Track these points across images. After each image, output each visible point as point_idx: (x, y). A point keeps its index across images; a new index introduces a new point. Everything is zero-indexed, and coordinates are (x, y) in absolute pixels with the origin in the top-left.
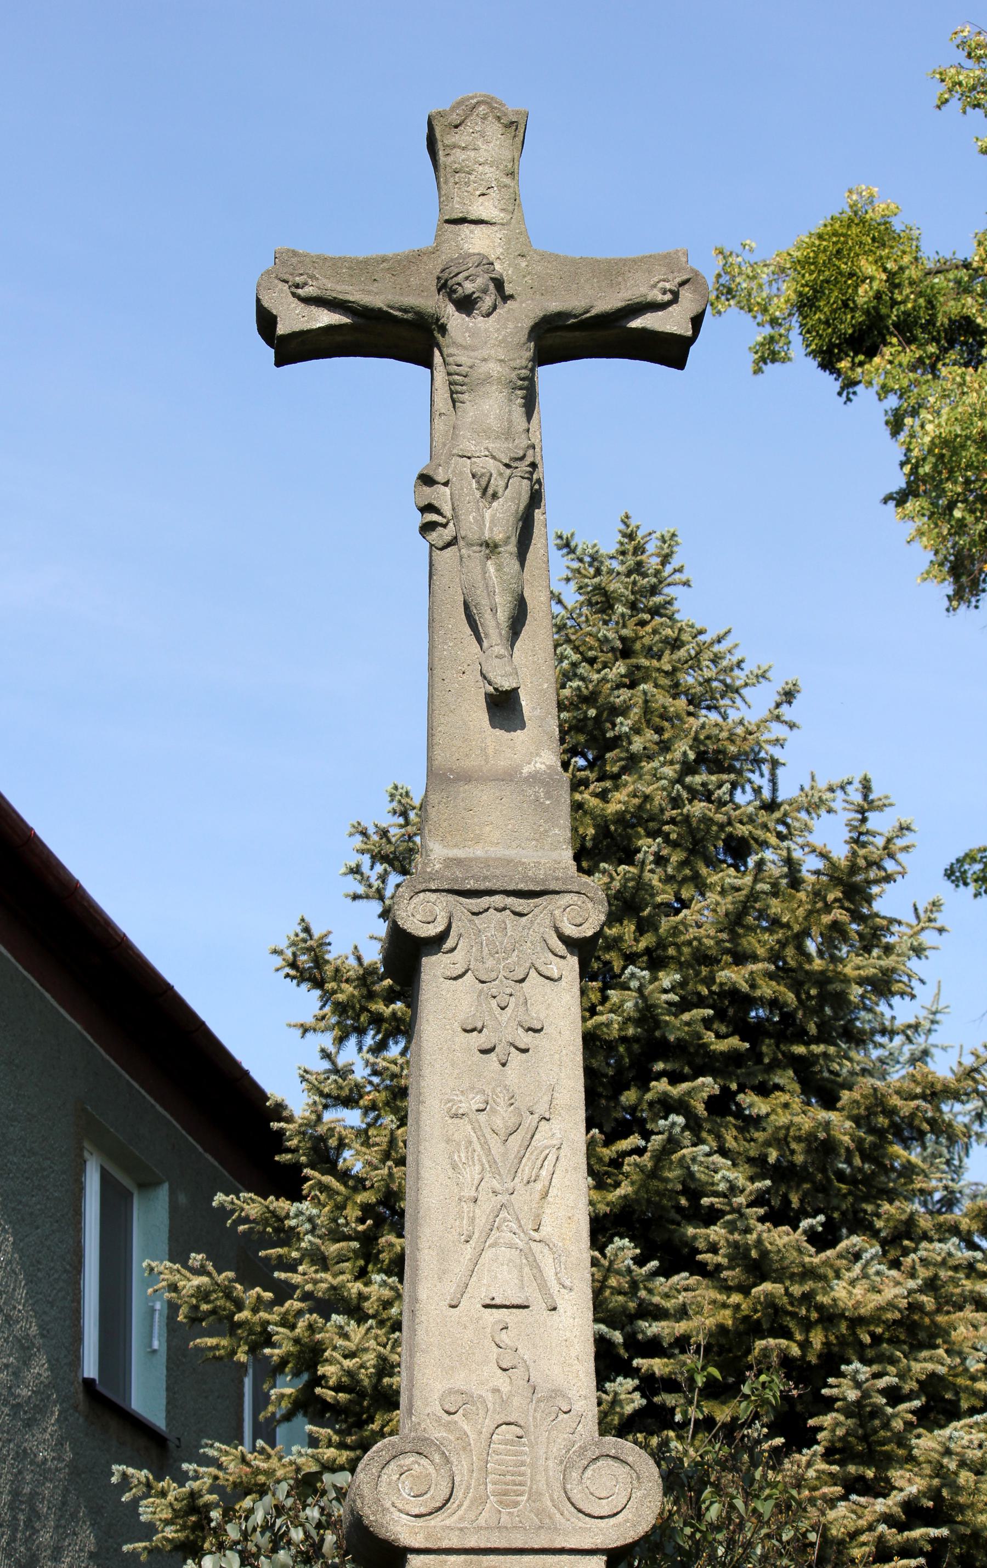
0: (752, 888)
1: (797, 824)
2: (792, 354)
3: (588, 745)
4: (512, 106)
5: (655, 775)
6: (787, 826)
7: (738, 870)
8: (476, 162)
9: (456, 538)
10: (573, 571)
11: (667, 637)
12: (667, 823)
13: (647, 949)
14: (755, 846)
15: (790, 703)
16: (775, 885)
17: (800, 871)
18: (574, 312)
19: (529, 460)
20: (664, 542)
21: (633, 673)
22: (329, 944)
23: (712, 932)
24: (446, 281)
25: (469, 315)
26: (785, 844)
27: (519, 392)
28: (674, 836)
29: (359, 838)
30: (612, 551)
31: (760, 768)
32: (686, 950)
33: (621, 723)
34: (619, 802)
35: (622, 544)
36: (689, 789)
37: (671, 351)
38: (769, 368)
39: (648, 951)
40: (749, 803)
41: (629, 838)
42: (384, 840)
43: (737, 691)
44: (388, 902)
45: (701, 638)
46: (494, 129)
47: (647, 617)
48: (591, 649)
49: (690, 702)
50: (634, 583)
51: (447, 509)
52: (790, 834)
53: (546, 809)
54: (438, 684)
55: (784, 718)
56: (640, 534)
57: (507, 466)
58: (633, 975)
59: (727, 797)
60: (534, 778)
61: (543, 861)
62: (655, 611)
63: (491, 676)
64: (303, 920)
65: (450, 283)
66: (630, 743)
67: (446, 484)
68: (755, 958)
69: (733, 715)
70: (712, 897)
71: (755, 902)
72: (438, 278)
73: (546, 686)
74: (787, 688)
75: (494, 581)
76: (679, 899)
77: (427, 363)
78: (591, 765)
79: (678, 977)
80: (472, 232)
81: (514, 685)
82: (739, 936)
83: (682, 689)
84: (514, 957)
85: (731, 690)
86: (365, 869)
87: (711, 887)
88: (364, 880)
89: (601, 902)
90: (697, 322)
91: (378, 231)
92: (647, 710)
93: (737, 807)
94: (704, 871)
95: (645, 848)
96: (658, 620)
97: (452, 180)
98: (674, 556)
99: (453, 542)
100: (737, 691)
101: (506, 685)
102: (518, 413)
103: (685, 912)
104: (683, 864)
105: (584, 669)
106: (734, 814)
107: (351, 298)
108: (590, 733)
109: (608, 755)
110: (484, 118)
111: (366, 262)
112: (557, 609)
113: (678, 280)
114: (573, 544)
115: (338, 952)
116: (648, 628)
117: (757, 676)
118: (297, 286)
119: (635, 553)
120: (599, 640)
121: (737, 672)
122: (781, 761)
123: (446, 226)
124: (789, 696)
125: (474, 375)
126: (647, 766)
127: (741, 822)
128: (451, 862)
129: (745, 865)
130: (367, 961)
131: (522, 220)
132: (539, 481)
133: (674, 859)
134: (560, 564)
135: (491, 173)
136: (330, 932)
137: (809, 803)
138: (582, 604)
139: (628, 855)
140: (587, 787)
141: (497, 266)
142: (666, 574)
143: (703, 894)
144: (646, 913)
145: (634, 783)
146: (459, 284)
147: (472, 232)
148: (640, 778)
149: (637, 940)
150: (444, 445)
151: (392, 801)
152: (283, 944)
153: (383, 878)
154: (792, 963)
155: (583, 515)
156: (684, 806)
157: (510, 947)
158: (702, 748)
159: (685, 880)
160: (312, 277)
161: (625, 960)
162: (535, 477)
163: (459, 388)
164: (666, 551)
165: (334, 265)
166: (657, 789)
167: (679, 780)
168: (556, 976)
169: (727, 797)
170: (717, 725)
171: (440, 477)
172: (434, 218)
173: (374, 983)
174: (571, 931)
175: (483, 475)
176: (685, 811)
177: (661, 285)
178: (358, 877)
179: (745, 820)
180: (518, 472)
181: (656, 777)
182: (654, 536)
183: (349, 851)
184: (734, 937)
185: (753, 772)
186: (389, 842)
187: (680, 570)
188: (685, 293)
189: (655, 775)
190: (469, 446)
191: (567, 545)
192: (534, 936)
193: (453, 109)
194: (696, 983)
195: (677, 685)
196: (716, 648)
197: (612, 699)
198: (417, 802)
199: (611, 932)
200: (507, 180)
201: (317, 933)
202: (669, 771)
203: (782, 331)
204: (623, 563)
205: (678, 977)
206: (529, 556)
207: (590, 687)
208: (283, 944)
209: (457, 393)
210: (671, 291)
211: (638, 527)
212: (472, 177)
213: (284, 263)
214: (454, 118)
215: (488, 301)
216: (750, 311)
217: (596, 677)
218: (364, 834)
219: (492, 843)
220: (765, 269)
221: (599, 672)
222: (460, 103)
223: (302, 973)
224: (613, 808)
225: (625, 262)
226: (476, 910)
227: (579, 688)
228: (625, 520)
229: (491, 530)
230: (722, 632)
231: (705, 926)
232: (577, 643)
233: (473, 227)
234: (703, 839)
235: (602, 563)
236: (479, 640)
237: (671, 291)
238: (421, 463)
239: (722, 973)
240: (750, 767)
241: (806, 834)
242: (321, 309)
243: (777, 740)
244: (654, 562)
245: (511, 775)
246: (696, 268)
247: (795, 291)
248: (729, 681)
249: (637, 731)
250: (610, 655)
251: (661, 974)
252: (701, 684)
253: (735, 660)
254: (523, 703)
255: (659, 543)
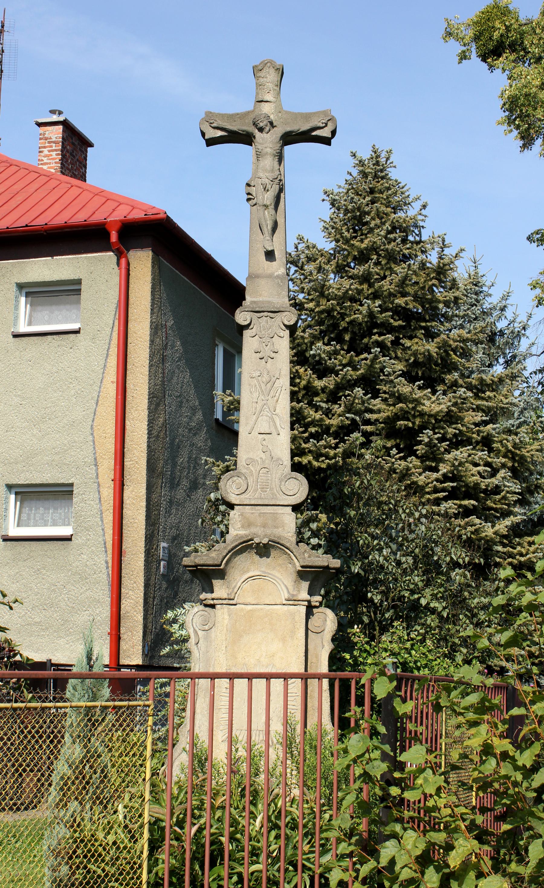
4: (279, 63)
19: (279, 178)
46: (272, 71)
51: (254, 194)
60: (278, 277)
99: (255, 204)
101: (270, 249)
102: (276, 163)
128: (253, 302)
132: (282, 185)
135: (270, 85)
165: (223, 116)
171: (252, 185)
172: (253, 100)
174: (287, 323)
188: (330, 124)
190: (261, 175)
193: (260, 64)
214: (260, 68)
222: (262, 63)
225: (311, 113)
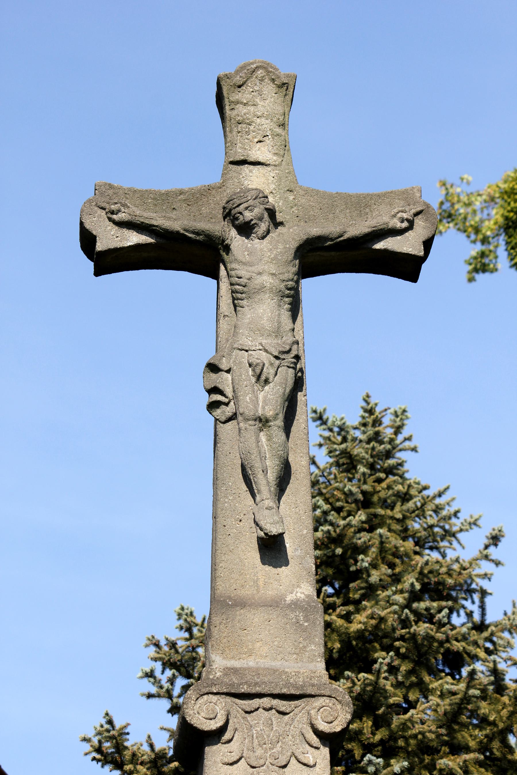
0: (466, 693)
1: (501, 642)
2: (499, 266)
3: (335, 577)
4: (284, 70)
5: (388, 602)
6: (494, 643)
7: (454, 678)
8: (255, 115)
9: (235, 414)
10: (325, 438)
11: (398, 492)
12: (398, 640)
13: (382, 740)
14: (467, 659)
15: (496, 545)
16: (484, 691)
17: (503, 680)
18: (331, 236)
19: (294, 353)
20: (397, 416)
21: (371, 520)
22: (128, 734)
23: (433, 728)
24: (230, 210)
25: (248, 237)
26: (492, 657)
27: (287, 300)
28: (403, 650)
29: (153, 649)
30: (356, 423)
31: (471, 597)
32: (412, 742)
33: (363, 560)
34: (359, 622)
35: (363, 417)
36: (415, 612)
37: (407, 268)
38: (480, 277)
39: (382, 742)
40: (463, 625)
41: (367, 651)
42: (173, 651)
43: (454, 535)
44: (175, 700)
45: (425, 493)
46: (269, 89)
47: (382, 475)
48: (338, 500)
49: (417, 544)
50: (373, 449)
51: (229, 392)
52: (496, 649)
53: (305, 630)
54: (220, 530)
55: (492, 557)
56: (378, 410)
57: (277, 358)
58: (370, 762)
59: (446, 620)
60: (296, 605)
61: (302, 671)
62: (390, 471)
63: (262, 523)
64: (107, 714)
65: (233, 212)
66: (369, 575)
67: (228, 371)
68: (467, 749)
69: (451, 555)
70: (434, 700)
71: (468, 704)
72: (224, 208)
73: (305, 532)
74: (494, 533)
75: (265, 450)
76: (406, 699)
77: (215, 275)
78: (337, 593)
79: (406, 764)
80: (251, 171)
81: (281, 531)
82: (455, 731)
83: (410, 533)
84: (278, 748)
85: (449, 534)
86: (158, 673)
87: (433, 691)
88: (157, 682)
89: (348, 705)
90: (428, 244)
91: (176, 168)
92: (382, 549)
93: (454, 628)
94: (427, 678)
95: (380, 660)
96: (391, 478)
97: (235, 130)
98: (405, 428)
99: (233, 417)
100: (454, 535)
101: (274, 530)
102: (286, 316)
103: (412, 711)
104: (410, 673)
105: (332, 516)
106: (451, 633)
107: (155, 223)
108: (337, 568)
109: (351, 585)
110: (262, 80)
111: (167, 194)
112: (313, 468)
113: (413, 211)
114: (325, 417)
115: (135, 740)
116: (384, 485)
117: (470, 524)
118: (113, 213)
119: (374, 425)
120: (345, 493)
121: (454, 520)
122: (489, 591)
123: (231, 166)
124: (495, 539)
125: (252, 285)
126: (382, 594)
127: (457, 640)
128: (229, 671)
129: (460, 673)
130: (158, 747)
131: (290, 163)
132: (301, 370)
133: (403, 668)
134: (316, 433)
135: (266, 125)
136: (128, 724)
137: (511, 625)
138: (331, 465)
139: (367, 665)
140: (334, 610)
141: (271, 199)
142: (398, 442)
143: (426, 697)
144: (381, 711)
145: (371, 607)
146: (241, 213)
147: (251, 171)
148: (377, 603)
149: (373, 734)
150: (227, 340)
151: (179, 619)
152: (91, 733)
153: (172, 681)
154: (498, 754)
155: (335, 394)
156: (412, 626)
157: (275, 739)
158: (426, 580)
159: (412, 685)
160: (124, 205)
161: (364, 749)
162: (298, 366)
163: (239, 296)
164: (398, 423)
165: (142, 196)
166: (390, 613)
167: (408, 606)
168: (311, 763)
169: (446, 620)
170: (437, 562)
171: (224, 365)
172: (221, 160)
173: (163, 765)
174: (323, 727)
175: (257, 364)
176: (412, 630)
177: (400, 215)
178: (152, 680)
179: (460, 638)
180: (285, 363)
181: (389, 603)
182: (389, 411)
183: (145, 659)
184: (451, 732)
185: (466, 599)
186: (177, 652)
187: (409, 439)
188: (419, 222)
189: (388, 602)
190: (246, 341)
191: (320, 418)
192: (294, 731)
193: (237, 72)
194: (420, 769)
195: (406, 530)
196: (438, 501)
197: (355, 540)
198: (199, 621)
199: (354, 726)
200: (279, 130)
201: (118, 724)
202: (399, 598)
203: (492, 248)
204: (364, 433)
205: (406, 764)
206: (293, 429)
207: (338, 530)
208: (91, 733)
209: (238, 299)
210: (408, 220)
211: (376, 404)
212: (252, 128)
213: (102, 194)
214: (238, 80)
215: (263, 227)
216: (465, 231)
217: (342, 523)
218: (157, 645)
219: (261, 656)
220: (479, 198)
221: (344, 518)
222: (242, 68)
223: (105, 757)
224: (354, 627)
225: (371, 196)
226: (248, 709)
227: (328, 532)
228: (367, 399)
229: (263, 408)
230: (442, 488)
231: (429, 723)
232: (327, 496)
233: (251, 167)
234: (426, 653)
235: (348, 432)
236: (253, 495)
237: (407, 220)
238: (209, 354)
239: (442, 761)
240: (464, 596)
241: (508, 649)
242: (131, 231)
243: (486, 575)
244: (389, 432)
245: (277, 602)
246: (428, 201)
247: (503, 215)
248: (447, 527)
249: (374, 566)
250: (353, 505)
251: (393, 761)
252: (425, 529)
253: (452, 510)
254: (287, 545)
255: (393, 417)
